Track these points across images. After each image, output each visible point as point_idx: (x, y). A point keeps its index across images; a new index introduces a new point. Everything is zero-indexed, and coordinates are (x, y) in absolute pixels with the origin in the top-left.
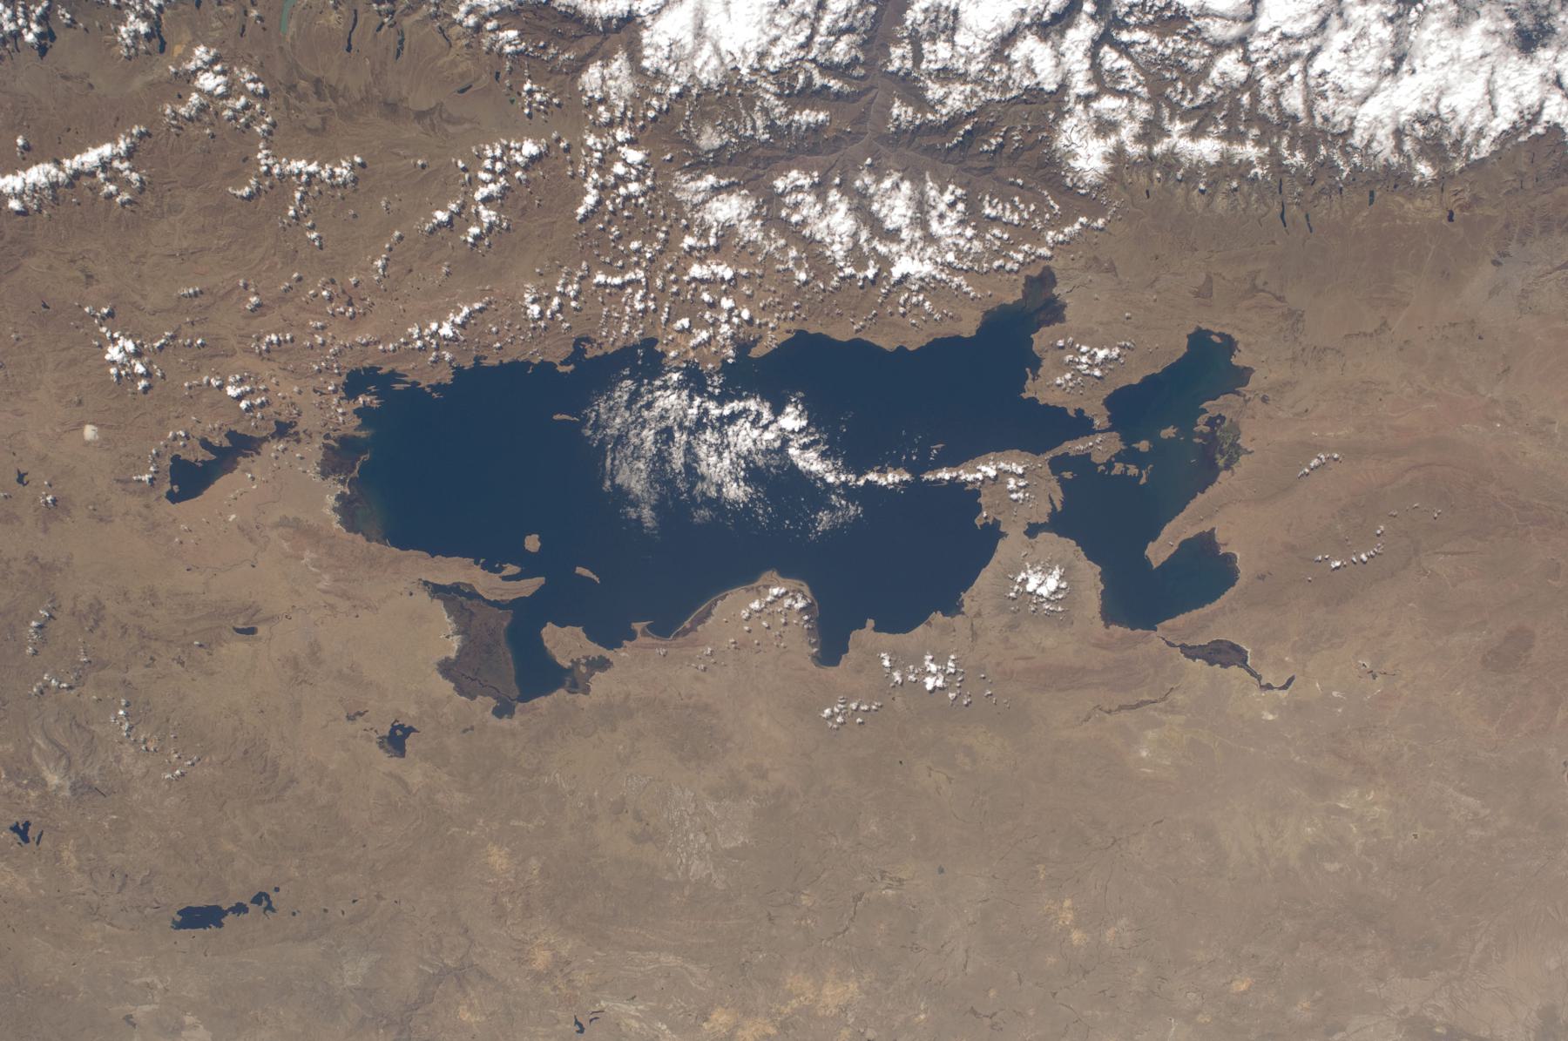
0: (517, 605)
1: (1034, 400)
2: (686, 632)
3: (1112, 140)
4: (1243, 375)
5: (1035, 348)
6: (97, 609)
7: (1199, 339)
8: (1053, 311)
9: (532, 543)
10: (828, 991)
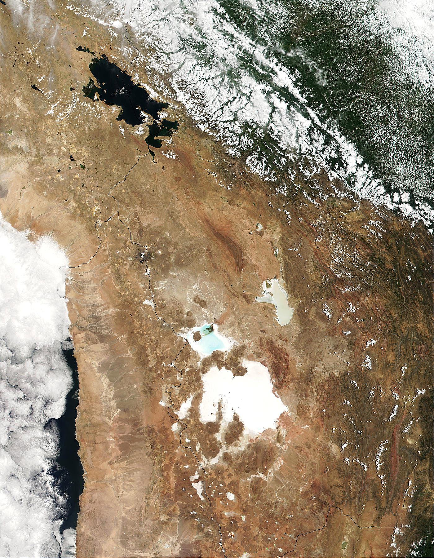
6: (59, 51)
7: (176, 122)
9: (104, 84)
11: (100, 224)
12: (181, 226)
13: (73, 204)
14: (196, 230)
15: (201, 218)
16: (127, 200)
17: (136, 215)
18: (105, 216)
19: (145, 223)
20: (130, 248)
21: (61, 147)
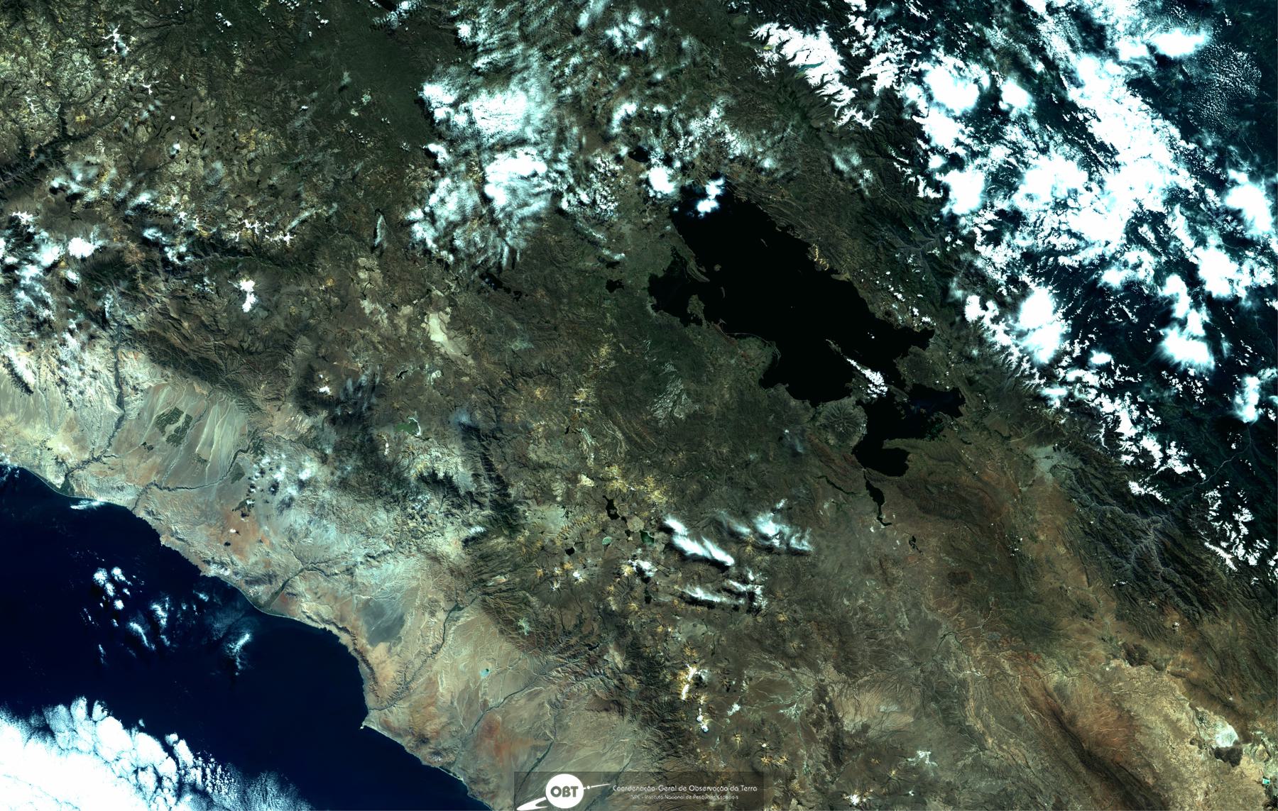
0: (695, 281)
1: (895, 364)
2: (733, 336)
3: (983, 313)
4: (959, 414)
5: (910, 350)
7: (956, 391)
8: (924, 345)
9: (717, 268)
10: (656, 493)
11: (704, 723)
12: (970, 731)
13: (616, 658)
14: (1018, 745)
15: (1034, 705)
16: (794, 645)
17: (821, 693)
18: (719, 699)
19: (851, 721)
20: (804, 802)
21: (576, 474)
